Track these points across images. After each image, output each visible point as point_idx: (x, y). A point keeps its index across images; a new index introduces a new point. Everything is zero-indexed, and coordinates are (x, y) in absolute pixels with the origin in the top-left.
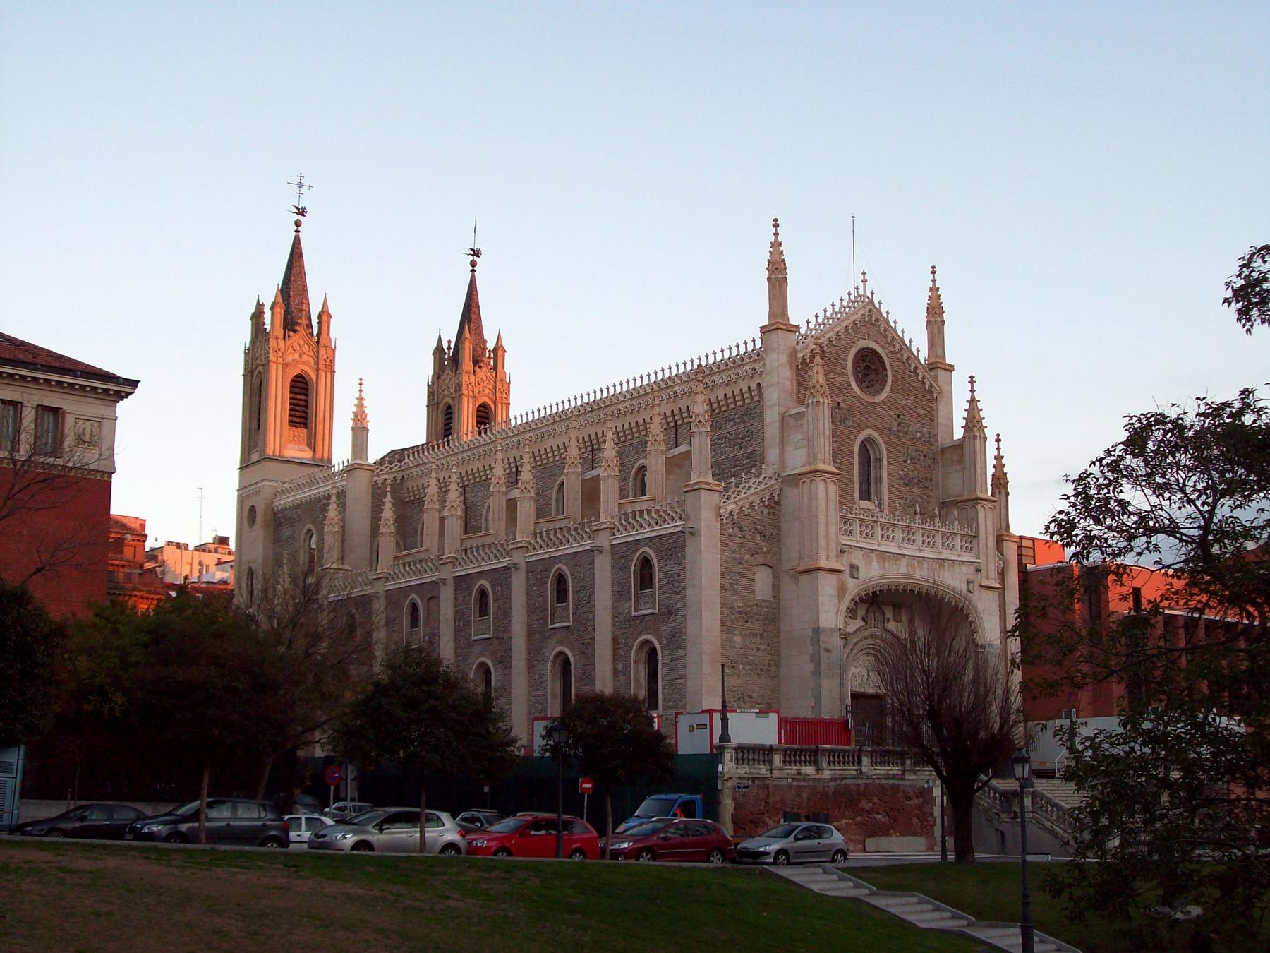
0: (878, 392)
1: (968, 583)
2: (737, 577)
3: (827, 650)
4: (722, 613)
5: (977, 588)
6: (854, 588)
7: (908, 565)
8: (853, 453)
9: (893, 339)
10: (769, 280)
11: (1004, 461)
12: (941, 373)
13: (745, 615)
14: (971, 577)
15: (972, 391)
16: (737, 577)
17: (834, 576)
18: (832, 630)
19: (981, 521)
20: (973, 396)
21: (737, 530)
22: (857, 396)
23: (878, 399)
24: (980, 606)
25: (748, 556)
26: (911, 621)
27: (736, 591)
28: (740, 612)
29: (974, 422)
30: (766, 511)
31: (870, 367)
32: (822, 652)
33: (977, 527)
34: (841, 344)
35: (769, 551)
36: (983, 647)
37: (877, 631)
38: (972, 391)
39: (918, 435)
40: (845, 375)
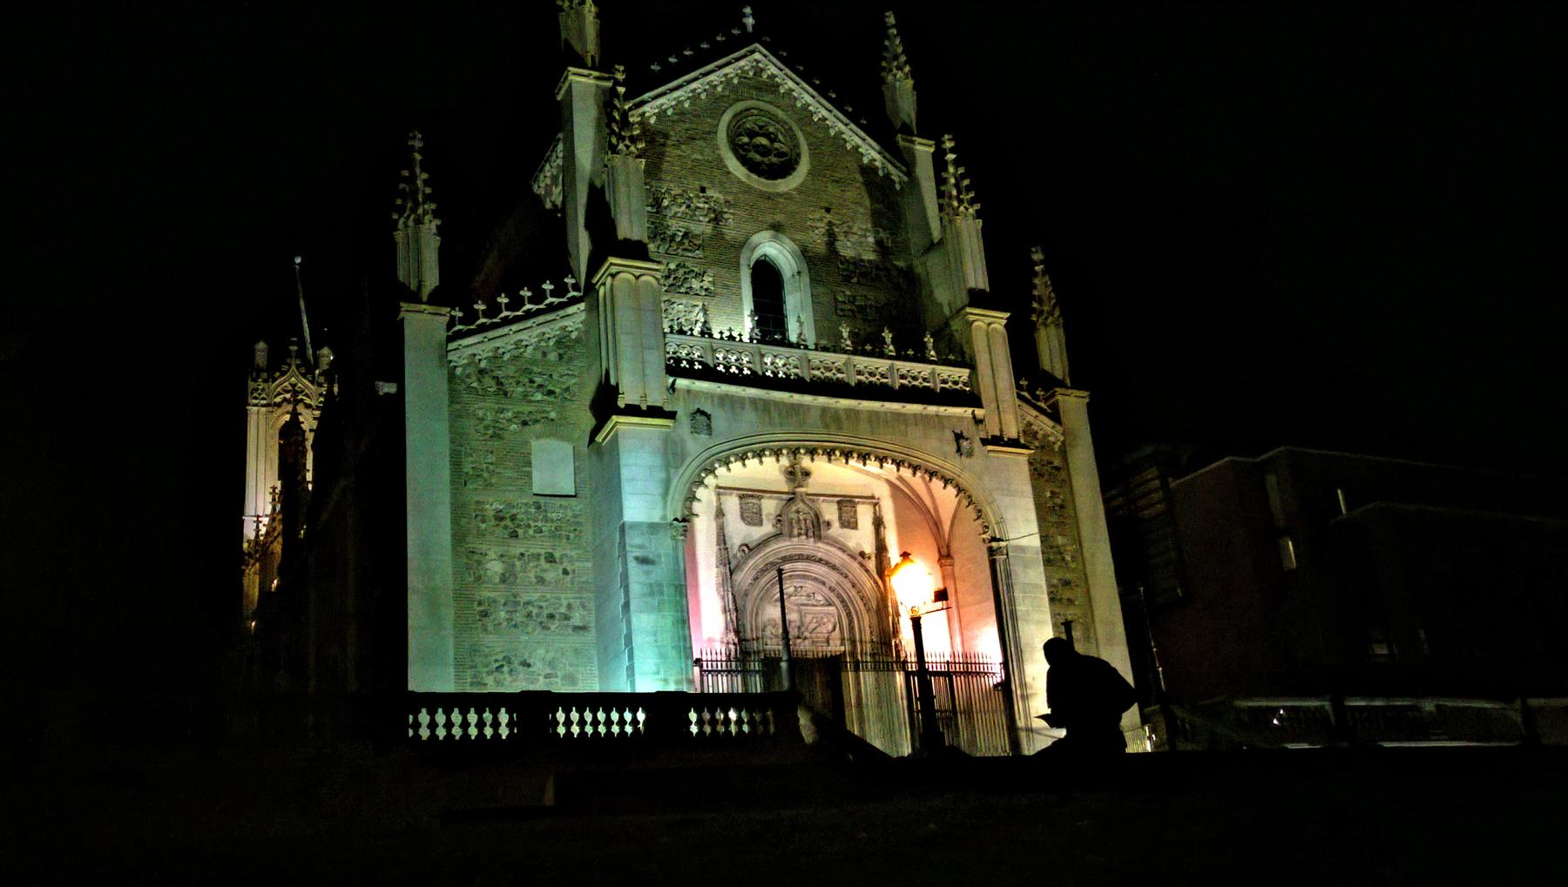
25: (513, 427)
26: (878, 523)
32: (632, 564)
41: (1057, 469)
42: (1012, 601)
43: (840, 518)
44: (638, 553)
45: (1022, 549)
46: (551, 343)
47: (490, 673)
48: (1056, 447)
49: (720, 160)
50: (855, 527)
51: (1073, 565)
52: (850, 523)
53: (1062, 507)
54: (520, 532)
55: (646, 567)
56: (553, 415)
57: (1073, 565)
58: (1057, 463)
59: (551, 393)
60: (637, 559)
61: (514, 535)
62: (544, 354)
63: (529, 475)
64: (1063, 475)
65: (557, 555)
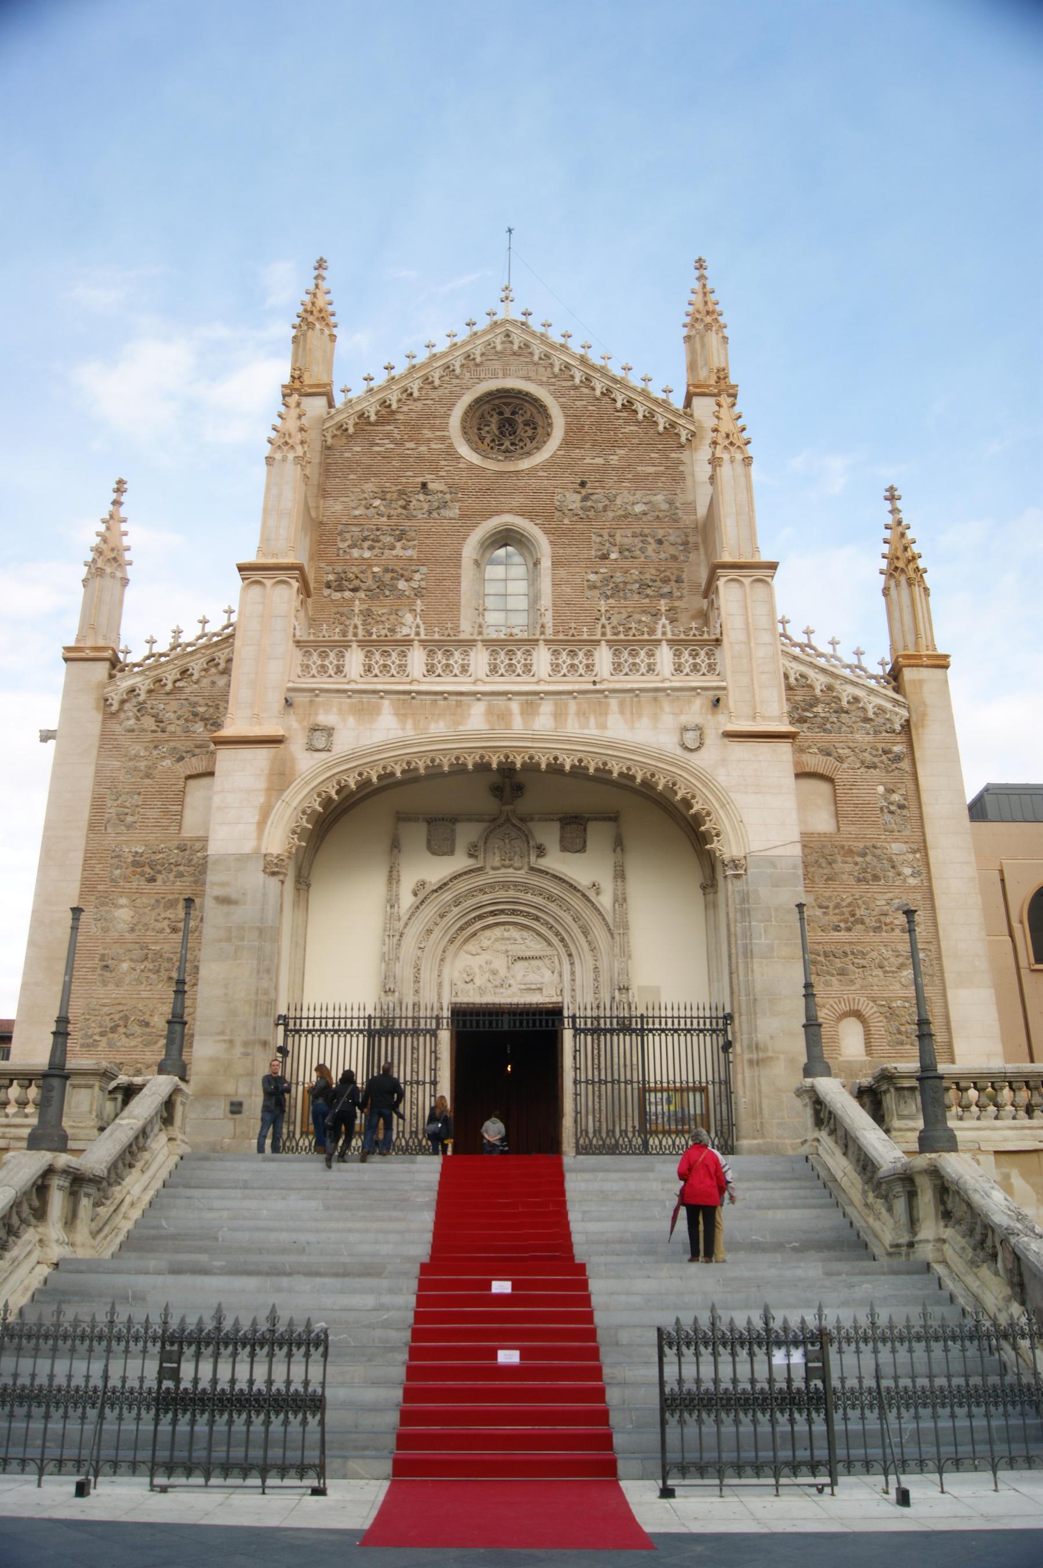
0: (529, 454)
2: (137, 800)
3: (225, 901)
4: (87, 866)
6: (313, 774)
7: (490, 712)
8: (456, 560)
9: (568, 366)
11: (910, 534)
13: (147, 868)
14: (686, 719)
16: (137, 800)
17: (262, 756)
18: (243, 859)
21: (149, 722)
22: (471, 466)
23: (525, 464)
24: (722, 778)
25: (167, 763)
27: (129, 827)
28: (136, 864)
31: (506, 420)
34: (434, 395)
36: (735, 864)
39: (638, 508)
40: (443, 439)
41: (898, 758)
42: (747, 933)
43: (561, 841)
45: (771, 862)
47: (102, 1034)
48: (897, 727)
49: (451, 446)
50: (582, 849)
51: (912, 881)
53: (901, 807)
54: (159, 877)
55: (225, 908)
57: (912, 881)
58: (897, 749)
61: (152, 880)
62: (213, 683)
63: (181, 813)
64: (905, 765)
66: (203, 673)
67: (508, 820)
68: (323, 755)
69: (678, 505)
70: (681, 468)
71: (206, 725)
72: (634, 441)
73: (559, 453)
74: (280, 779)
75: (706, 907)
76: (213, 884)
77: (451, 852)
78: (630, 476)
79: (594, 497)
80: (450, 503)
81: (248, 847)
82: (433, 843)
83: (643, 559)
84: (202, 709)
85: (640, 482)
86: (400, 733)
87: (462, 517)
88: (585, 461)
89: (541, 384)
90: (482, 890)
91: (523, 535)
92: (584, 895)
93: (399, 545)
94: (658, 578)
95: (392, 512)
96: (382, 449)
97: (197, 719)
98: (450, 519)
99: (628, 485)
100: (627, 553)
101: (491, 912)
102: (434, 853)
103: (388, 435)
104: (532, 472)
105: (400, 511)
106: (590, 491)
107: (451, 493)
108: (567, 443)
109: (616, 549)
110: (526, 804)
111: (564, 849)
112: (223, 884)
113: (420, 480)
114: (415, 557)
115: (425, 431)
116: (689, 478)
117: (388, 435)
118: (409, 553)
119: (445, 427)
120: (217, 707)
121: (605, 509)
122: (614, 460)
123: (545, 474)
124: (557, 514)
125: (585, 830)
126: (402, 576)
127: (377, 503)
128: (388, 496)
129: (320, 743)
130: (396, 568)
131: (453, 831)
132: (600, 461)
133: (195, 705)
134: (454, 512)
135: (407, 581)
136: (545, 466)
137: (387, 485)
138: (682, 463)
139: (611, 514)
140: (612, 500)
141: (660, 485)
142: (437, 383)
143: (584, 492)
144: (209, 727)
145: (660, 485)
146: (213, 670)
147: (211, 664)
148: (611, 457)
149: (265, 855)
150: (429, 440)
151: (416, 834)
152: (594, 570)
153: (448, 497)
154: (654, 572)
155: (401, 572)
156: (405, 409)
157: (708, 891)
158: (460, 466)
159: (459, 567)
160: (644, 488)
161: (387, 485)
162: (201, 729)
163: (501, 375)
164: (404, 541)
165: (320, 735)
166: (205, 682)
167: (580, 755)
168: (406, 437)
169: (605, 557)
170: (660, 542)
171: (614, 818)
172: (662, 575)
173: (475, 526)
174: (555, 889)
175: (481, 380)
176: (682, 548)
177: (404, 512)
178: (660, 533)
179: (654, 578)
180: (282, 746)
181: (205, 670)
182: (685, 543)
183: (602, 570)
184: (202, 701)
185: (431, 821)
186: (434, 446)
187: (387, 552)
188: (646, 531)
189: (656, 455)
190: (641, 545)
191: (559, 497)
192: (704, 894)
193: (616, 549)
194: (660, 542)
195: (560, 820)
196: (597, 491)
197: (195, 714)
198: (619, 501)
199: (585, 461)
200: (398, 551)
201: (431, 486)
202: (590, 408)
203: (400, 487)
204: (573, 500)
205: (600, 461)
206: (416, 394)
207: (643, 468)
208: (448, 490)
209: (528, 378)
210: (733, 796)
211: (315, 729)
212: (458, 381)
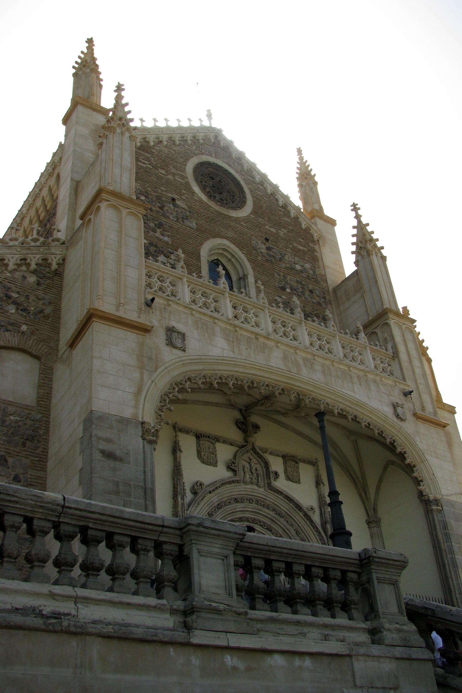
0: (234, 208)
1: (395, 406)
3: (109, 455)
5: (409, 417)
7: (285, 358)
10: (75, 75)
12: (320, 222)
15: (358, 217)
17: (131, 337)
19: (398, 339)
20: (359, 222)
22: (201, 201)
23: (233, 214)
29: (366, 245)
30: (32, 279)
33: (395, 347)
35: (32, 333)
36: (437, 502)
37: (261, 492)
38: (358, 217)
40: (183, 177)
43: (286, 471)
44: (103, 446)
46: (33, 267)
49: (187, 184)
50: (298, 481)
52: (293, 478)
55: (112, 463)
56: (24, 328)
59: (24, 310)
60: (103, 452)
62: (24, 277)
65: (10, 460)
66: (16, 267)
67: (254, 449)
68: (180, 353)
69: (317, 273)
70: (316, 254)
71: (17, 309)
72: (290, 227)
73: (251, 215)
74: (147, 362)
75: (372, 537)
76: (99, 438)
77: (215, 464)
78: (291, 246)
79: (274, 250)
80: (189, 217)
81: (128, 413)
82: (202, 454)
83: (304, 299)
84: (15, 295)
85: (296, 251)
86: (231, 355)
87: (197, 230)
88: (266, 227)
89: (237, 172)
90: (236, 500)
91: (233, 256)
92: (306, 515)
93: (158, 230)
94: (313, 314)
95: (154, 208)
96: (144, 166)
97: (10, 301)
98: (191, 228)
99: (290, 251)
100: (295, 292)
101: (241, 518)
102: (203, 462)
103: (148, 159)
104: (237, 220)
105: (158, 209)
106: (271, 246)
107: (190, 212)
108: (254, 212)
109: (288, 286)
110: (260, 440)
111: (288, 478)
112: (108, 441)
113: (170, 195)
114: (170, 243)
115: (171, 167)
116: (320, 261)
117: (148, 159)
118: (166, 239)
119: (184, 171)
120: (27, 297)
121: (280, 260)
122: (281, 234)
123: (245, 225)
124: (254, 252)
125: (298, 467)
126: (162, 252)
127: (143, 198)
128: (150, 196)
129: (179, 343)
130: (158, 245)
131: (215, 448)
132: (272, 230)
133: (9, 288)
134: (194, 225)
135: (165, 256)
136: (246, 219)
137: (149, 189)
138: (315, 251)
139: (283, 266)
140: (283, 256)
141: (307, 258)
142: (178, 143)
143: (267, 244)
144: (19, 311)
145: (307, 258)
146: (24, 268)
147: (23, 262)
148: (279, 231)
149: (143, 423)
150: (174, 175)
151: (188, 445)
152: (279, 295)
153: (188, 214)
154: (311, 308)
155: (161, 249)
156: (157, 148)
157: (372, 525)
158: (195, 198)
159: (200, 261)
160: (299, 257)
161: (149, 189)
162: (13, 311)
163: (214, 155)
164: (161, 230)
165: (174, 337)
166: (18, 275)
167: (342, 406)
168: (159, 165)
169: (284, 289)
170: (311, 291)
171: (313, 463)
172: (315, 312)
173: (207, 239)
174: (284, 506)
175: (202, 154)
176: (323, 300)
177: (160, 210)
178: (311, 287)
179: (311, 312)
180: (147, 335)
181: (17, 264)
182: (324, 298)
183: (283, 297)
184: (13, 288)
185: (198, 436)
186: (176, 178)
187: (152, 233)
188: (304, 283)
189: (302, 241)
190: (301, 290)
191: (254, 242)
192: (369, 528)
193: (288, 286)
194: (311, 291)
195: (284, 457)
196: (275, 247)
197: (9, 297)
198: (286, 258)
199: (266, 227)
200: (158, 234)
201: (178, 202)
202: (265, 198)
203: (157, 194)
204: (263, 248)
205: (272, 230)
206: (165, 143)
207: (297, 245)
208: (188, 209)
209: (230, 166)
210: (427, 457)
211: (170, 331)
212: (189, 148)
